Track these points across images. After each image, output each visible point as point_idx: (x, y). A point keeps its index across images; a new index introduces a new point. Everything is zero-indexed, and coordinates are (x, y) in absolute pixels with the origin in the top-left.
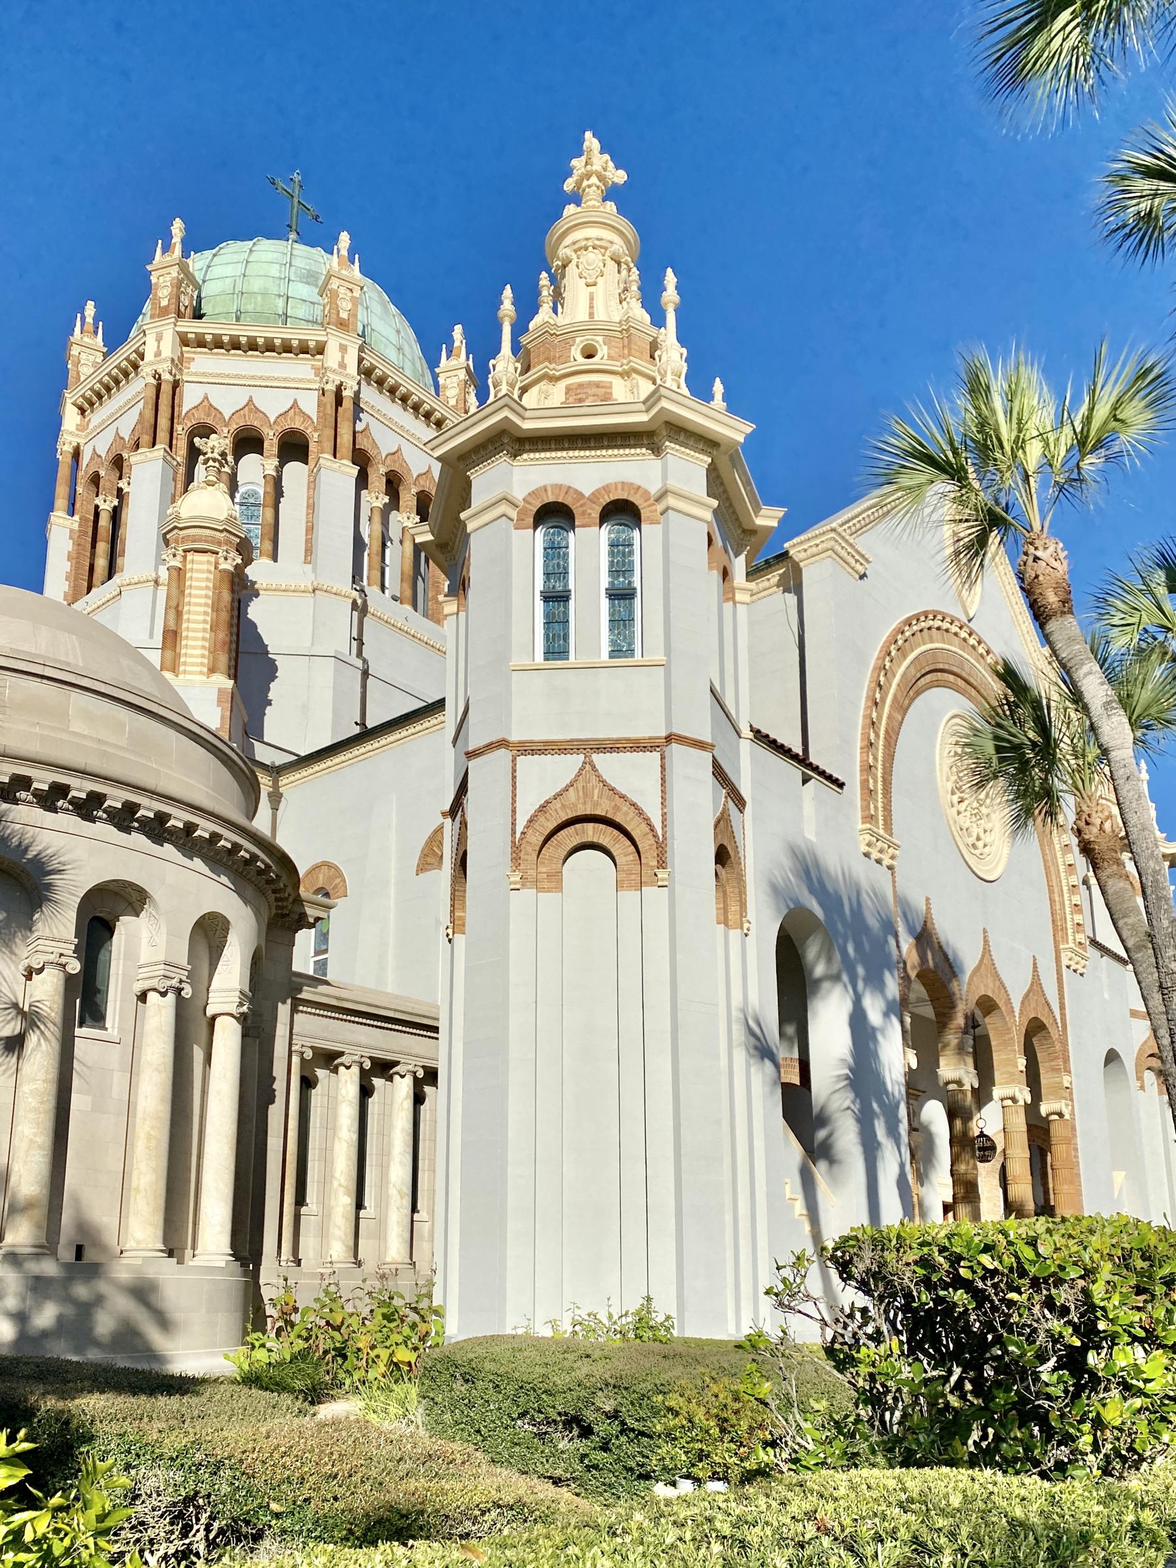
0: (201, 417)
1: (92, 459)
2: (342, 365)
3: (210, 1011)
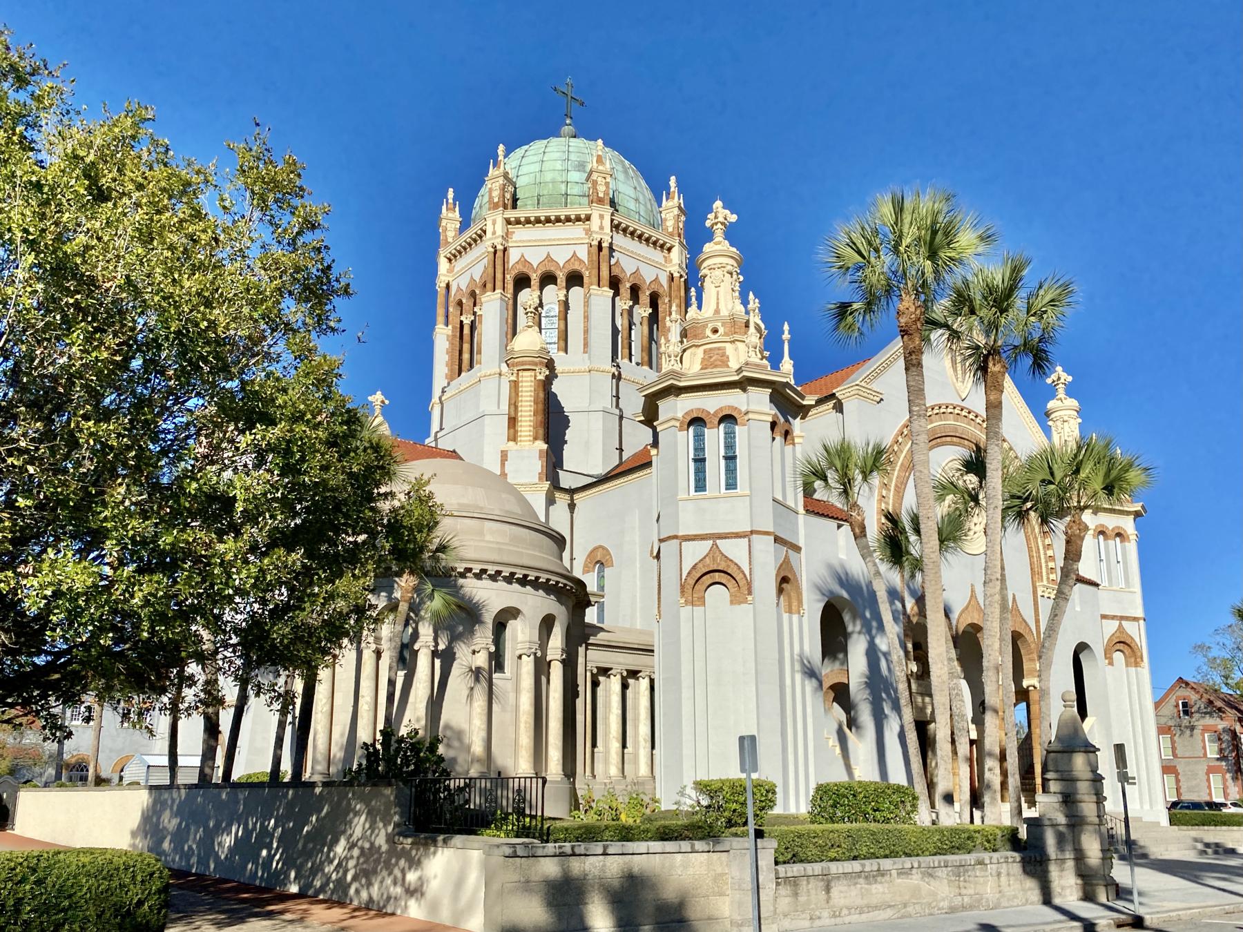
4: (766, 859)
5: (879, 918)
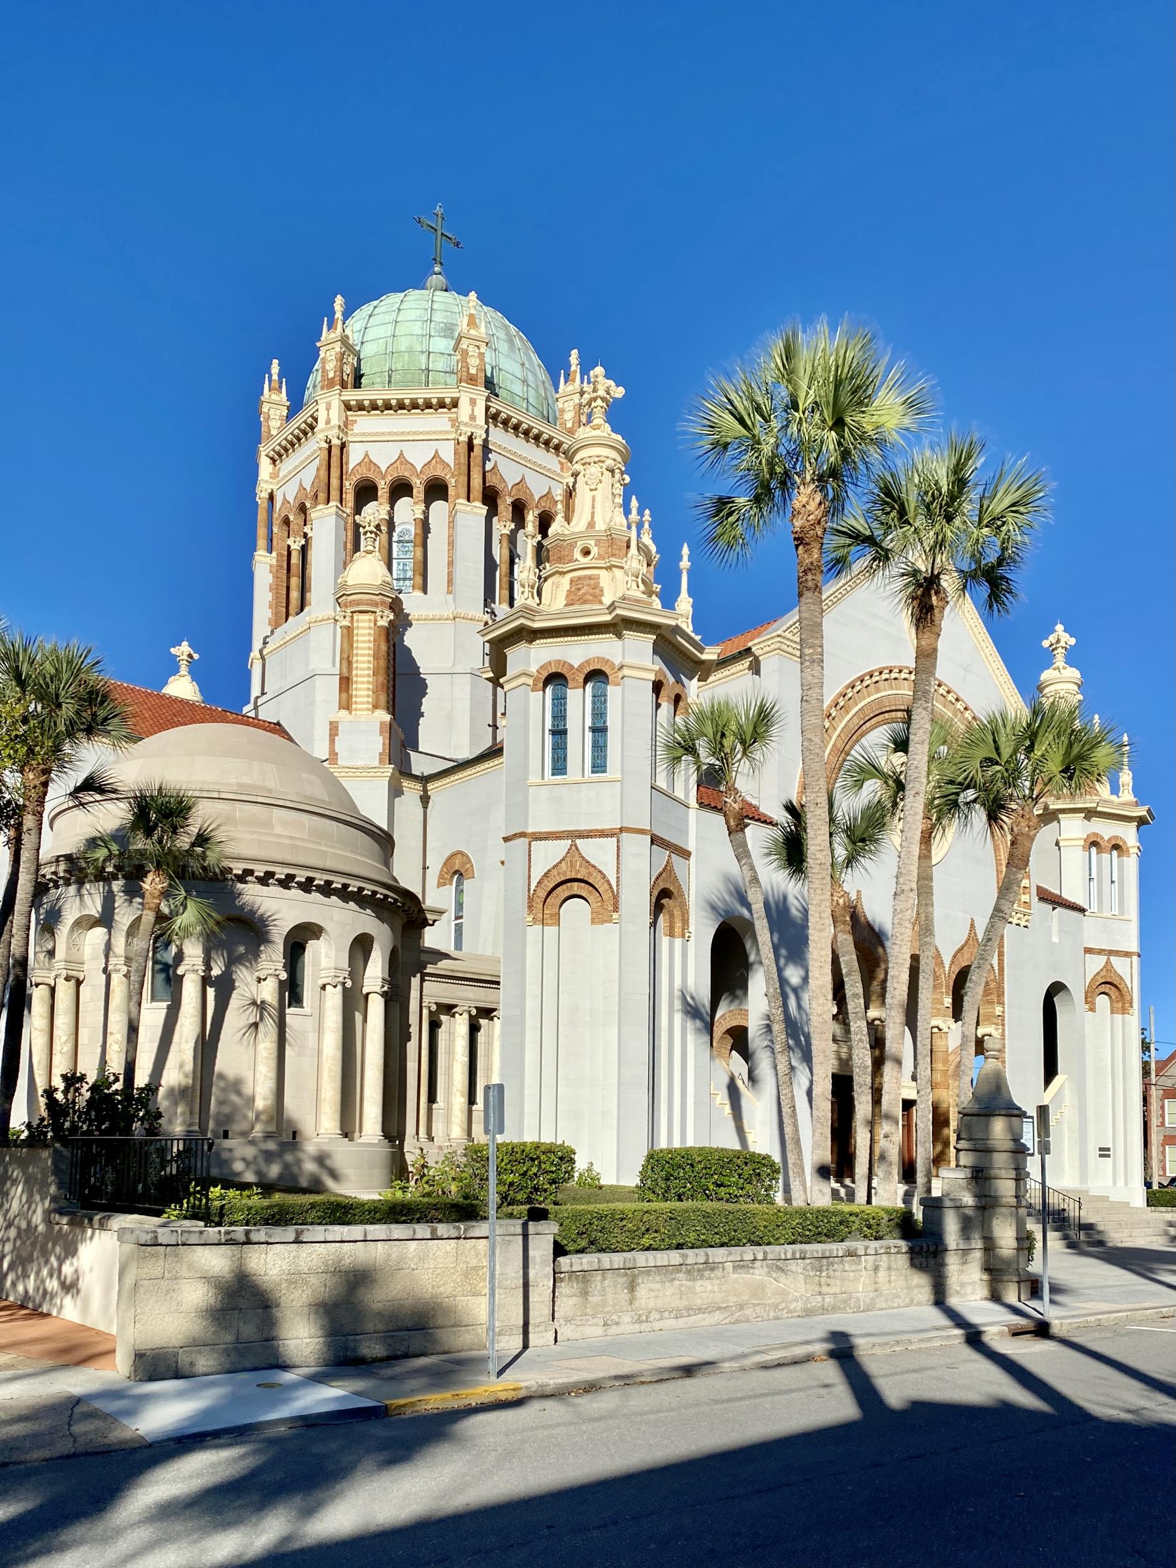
0: (364, 473)
1: (283, 504)
2: (473, 417)
3: (365, 991)
4: (541, 1248)
5: (704, 1323)
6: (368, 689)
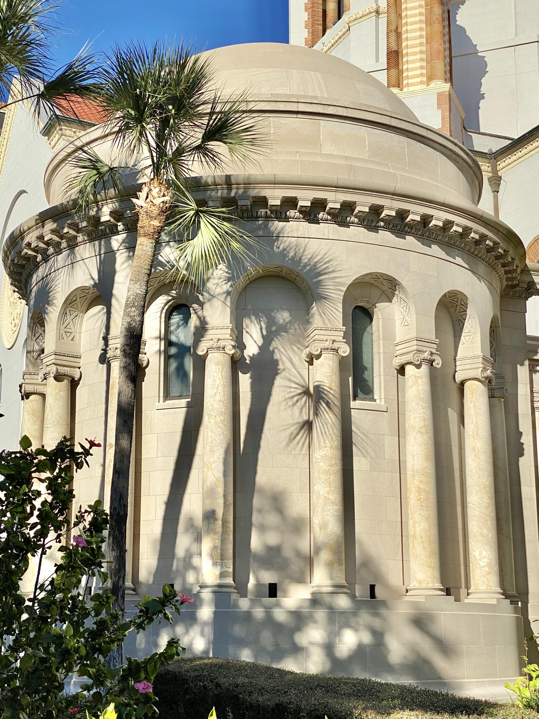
3: (459, 377)
6: (422, 60)
